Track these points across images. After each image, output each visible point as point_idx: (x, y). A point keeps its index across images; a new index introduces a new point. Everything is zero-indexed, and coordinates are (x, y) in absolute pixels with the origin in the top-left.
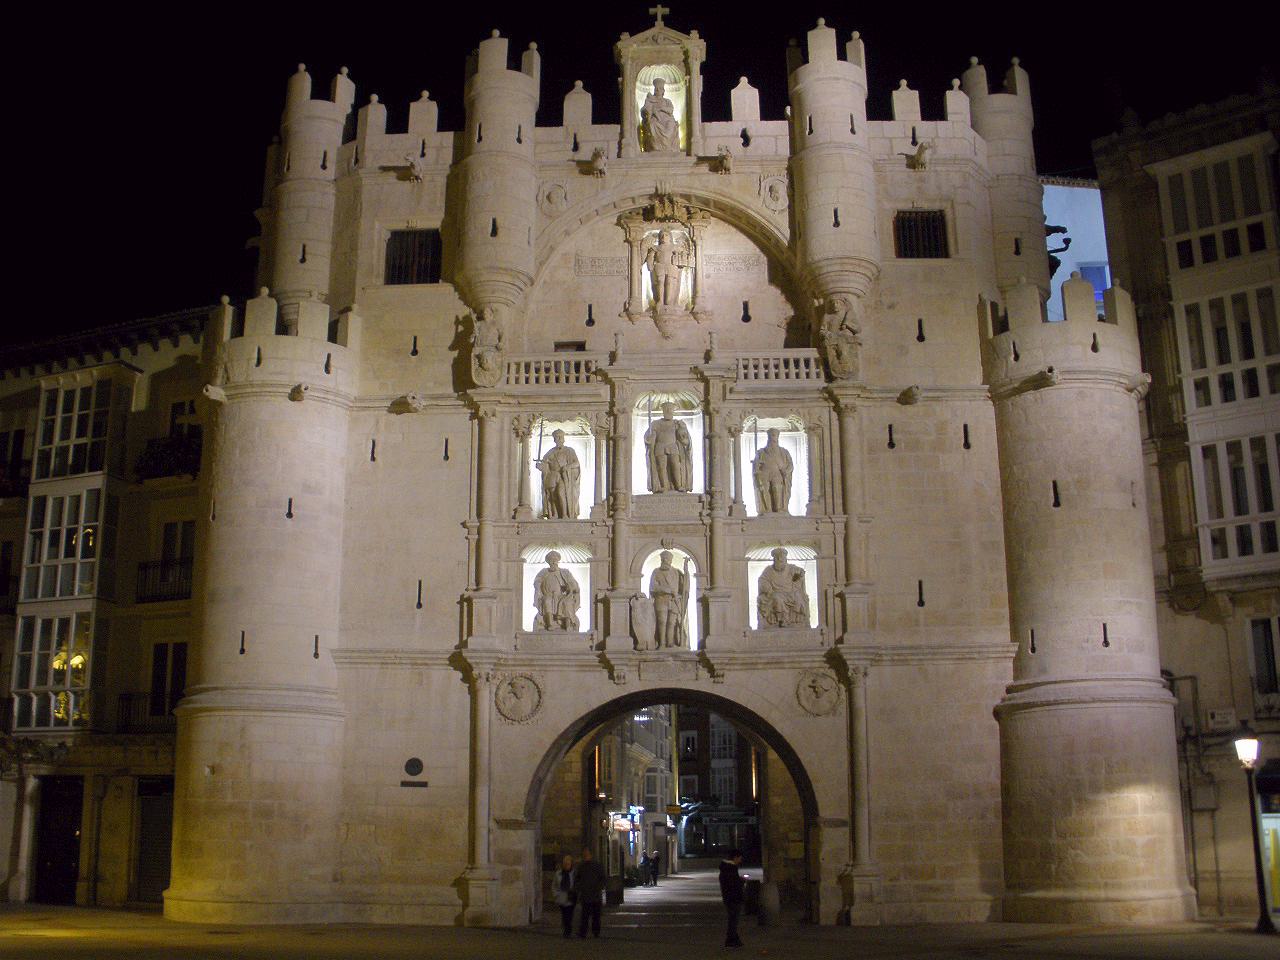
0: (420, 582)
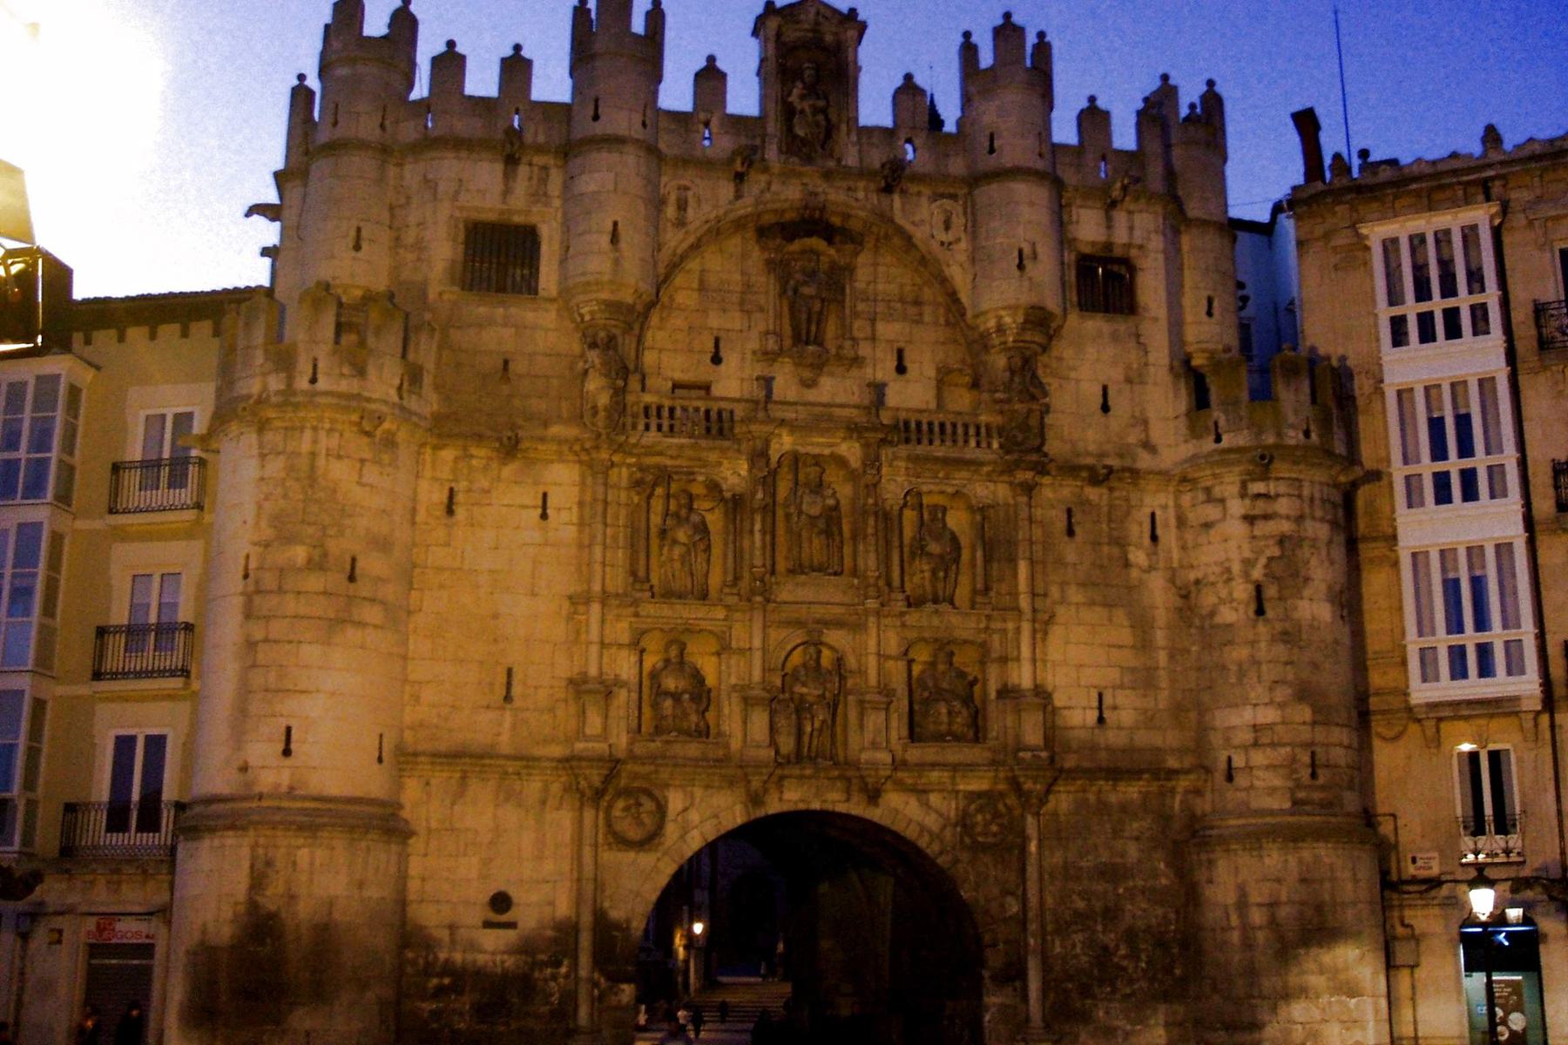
0: (510, 672)
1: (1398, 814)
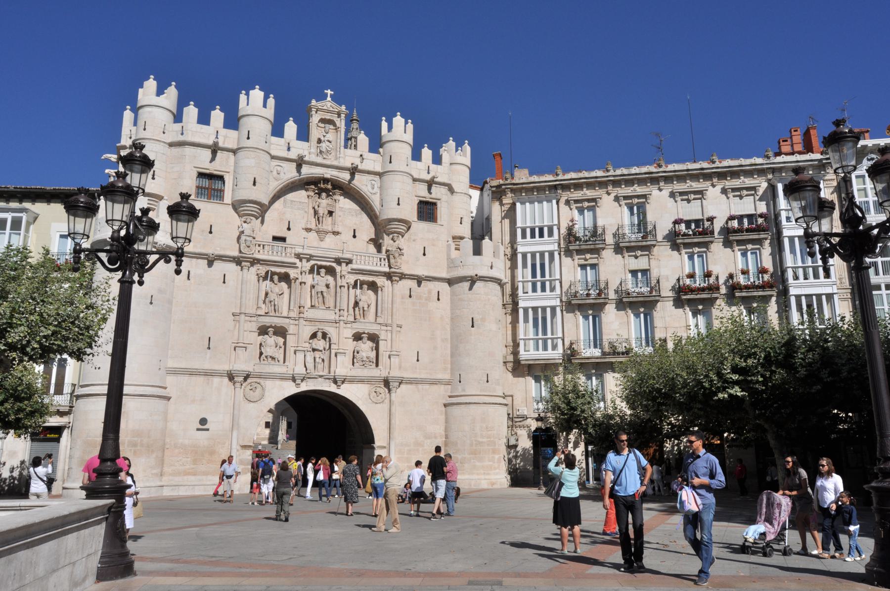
0: (210, 338)
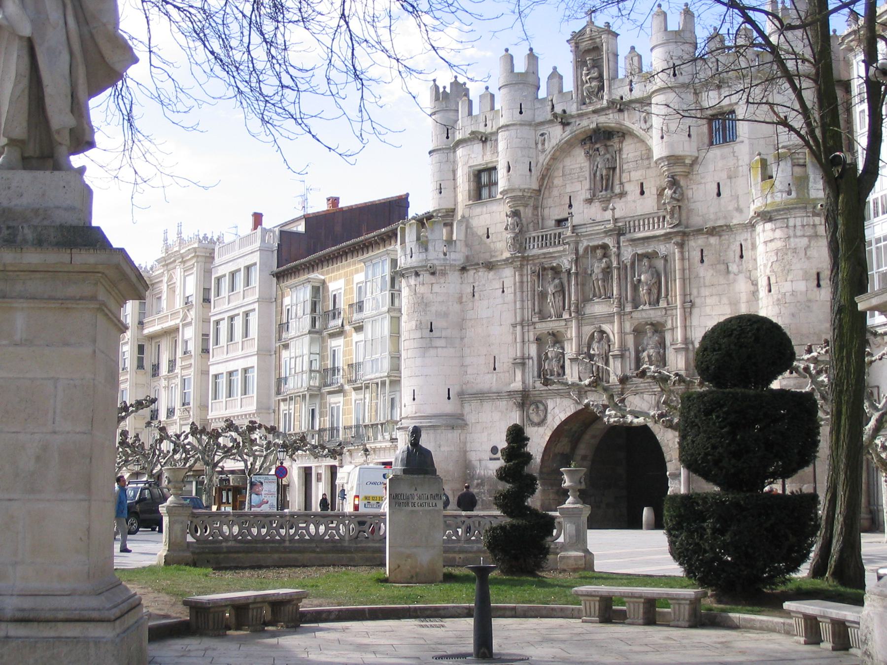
1: (880, 386)
